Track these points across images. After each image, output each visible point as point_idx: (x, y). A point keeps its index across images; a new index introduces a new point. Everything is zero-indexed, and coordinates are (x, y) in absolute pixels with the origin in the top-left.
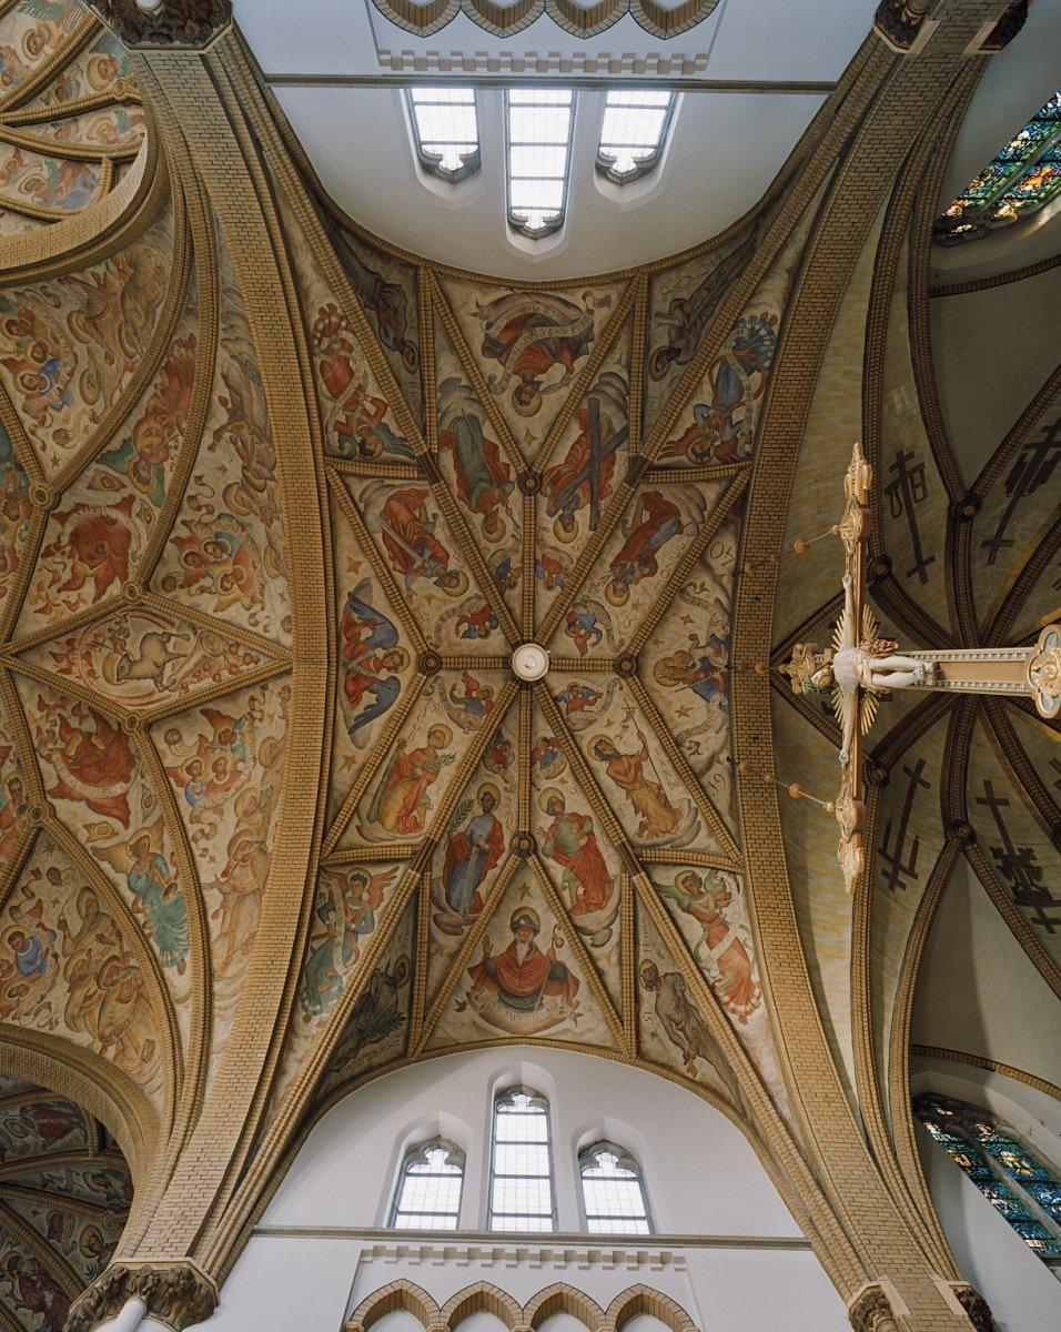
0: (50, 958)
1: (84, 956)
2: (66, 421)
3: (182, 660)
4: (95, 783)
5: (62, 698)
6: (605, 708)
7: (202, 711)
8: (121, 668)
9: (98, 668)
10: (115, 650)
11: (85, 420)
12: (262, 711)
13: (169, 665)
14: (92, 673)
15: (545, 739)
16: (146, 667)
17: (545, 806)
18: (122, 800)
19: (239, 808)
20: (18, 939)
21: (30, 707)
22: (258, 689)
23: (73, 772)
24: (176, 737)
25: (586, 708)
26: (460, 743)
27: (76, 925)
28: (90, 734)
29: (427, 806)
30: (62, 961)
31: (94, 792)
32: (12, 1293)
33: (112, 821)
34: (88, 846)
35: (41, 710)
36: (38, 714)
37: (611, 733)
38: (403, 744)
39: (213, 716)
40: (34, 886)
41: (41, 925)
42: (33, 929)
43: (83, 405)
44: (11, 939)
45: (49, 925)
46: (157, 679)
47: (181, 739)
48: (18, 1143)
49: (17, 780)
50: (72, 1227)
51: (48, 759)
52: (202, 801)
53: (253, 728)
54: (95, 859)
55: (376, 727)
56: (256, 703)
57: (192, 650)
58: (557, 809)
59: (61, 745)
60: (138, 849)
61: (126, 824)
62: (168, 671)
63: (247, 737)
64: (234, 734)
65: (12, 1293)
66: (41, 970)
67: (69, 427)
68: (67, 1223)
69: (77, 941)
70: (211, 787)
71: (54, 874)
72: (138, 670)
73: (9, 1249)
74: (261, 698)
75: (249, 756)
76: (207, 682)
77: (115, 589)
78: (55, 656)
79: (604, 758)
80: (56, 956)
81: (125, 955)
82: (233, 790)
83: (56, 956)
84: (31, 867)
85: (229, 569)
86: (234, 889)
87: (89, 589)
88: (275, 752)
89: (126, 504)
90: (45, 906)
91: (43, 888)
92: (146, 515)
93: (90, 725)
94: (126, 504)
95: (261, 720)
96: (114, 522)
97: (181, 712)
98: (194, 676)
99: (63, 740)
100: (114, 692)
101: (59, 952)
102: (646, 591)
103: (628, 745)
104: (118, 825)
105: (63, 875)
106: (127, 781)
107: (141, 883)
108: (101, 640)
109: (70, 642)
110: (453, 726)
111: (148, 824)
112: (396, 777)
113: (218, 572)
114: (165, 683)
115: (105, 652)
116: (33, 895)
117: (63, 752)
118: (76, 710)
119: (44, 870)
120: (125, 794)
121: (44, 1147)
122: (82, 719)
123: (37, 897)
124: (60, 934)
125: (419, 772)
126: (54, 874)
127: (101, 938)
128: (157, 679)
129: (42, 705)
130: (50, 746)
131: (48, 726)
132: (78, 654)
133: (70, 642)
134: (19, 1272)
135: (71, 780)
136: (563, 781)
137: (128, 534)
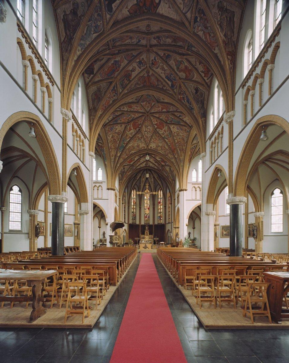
2: (175, 128)
11: (175, 131)
16: (147, 129)
27: (117, 131)
43: (176, 131)
46: (145, 131)
57: (149, 135)
60: (127, 135)
62: (146, 132)
67: (175, 129)
69: (116, 133)
72: (146, 128)
76: (145, 138)
77: (156, 127)
85: (157, 139)
87: (156, 123)
89: (165, 131)
92: (163, 134)
93: (139, 123)
94: (165, 131)
96: (163, 128)
100: (144, 127)
102: (153, 162)
103: (141, 161)
106: (133, 129)
113: (157, 138)
127: (117, 137)
128: (145, 131)
137: (162, 130)
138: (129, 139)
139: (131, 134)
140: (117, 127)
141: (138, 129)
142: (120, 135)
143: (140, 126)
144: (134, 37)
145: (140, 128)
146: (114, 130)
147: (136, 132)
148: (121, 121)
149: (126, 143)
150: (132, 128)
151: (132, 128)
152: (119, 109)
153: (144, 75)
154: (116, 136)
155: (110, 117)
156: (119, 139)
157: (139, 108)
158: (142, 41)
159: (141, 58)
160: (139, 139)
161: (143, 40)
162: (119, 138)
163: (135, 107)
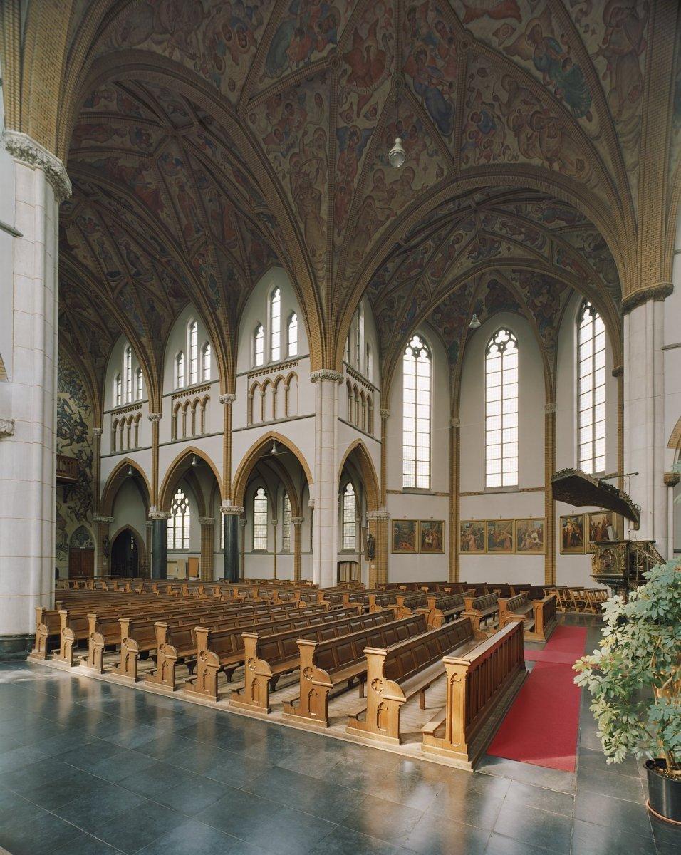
0: (496, 119)
20: (475, 117)
27: (504, 96)
30: (504, 120)
34: (501, 48)
41: (483, 103)
44: (472, 118)
45: (487, 101)
54: (509, 56)
66: (494, 128)
80: (498, 117)
83: (498, 117)
101: (499, 114)
105: (488, 71)
116: (474, 89)
123: (476, 88)
124: (496, 104)
140: (488, 97)
152: (369, 142)
155: (428, 144)
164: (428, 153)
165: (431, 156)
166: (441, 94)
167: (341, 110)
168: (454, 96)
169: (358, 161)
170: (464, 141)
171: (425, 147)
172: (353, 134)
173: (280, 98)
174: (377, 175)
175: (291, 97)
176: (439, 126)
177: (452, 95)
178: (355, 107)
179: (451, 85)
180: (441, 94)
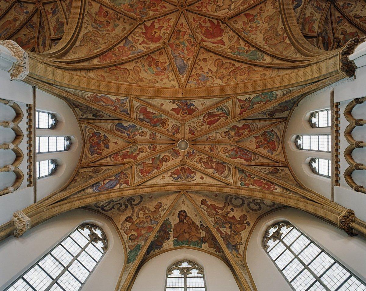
0: (208, 77)
1: (221, 74)
3: (237, 2)
4: (211, 38)
5: (200, 18)
6: (355, 7)
7: (244, 15)
8: (216, 9)
9: (209, 10)
10: (214, 4)
12: (264, 10)
13: (233, 5)
14: (208, 11)
15: (338, 17)
16: (225, 7)
17: (340, 33)
18: (222, 40)
19: (262, 33)
21: (192, 20)
22: (263, 4)
23: (204, 36)
24: (236, 22)
25: (349, 8)
26: (318, 16)
27: (214, 69)
28: (208, 27)
29: (315, 28)
31: (212, 40)
32: (202, 166)
33: (220, 45)
35: (194, 21)
36: (194, 23)
37: (358, 13)
38: (305, 15)
39: (247, 15)
40: (199, 63)
41: (203, 71)
42: (201, 73)
44: (196, 74)
45: (205, 71)
46: (229, 9)
47: (238, 23)
48: (199, 129)
49: (189, 39)
50: (217, 149)
51: (198, 33)
52: (249, 34)
53: (261, 16)
55: (299, 9)
56: (262, 9)
58: (344, 33)
59: (200, 30)
60: (230, 48)
61: (224, 45)
63: (259, 19)
64: (254, 19)
65: (202, 166)
68: (215, 148)
69: (217, 72)
70: (250, 31)
71: (205, 60)
73: (198, 157)
74: (264, 6)
75: (260, 22)
78: (198, 7)
79: (357, 18)
81: (238, 68)
82: (258, 30)
83: (211, 77)
84: (198, 58)
86: (271, 45)
88: (271, 18)
90: (203, 67)
91: (202, 64)
93: (208, 25)
95: (264, 13)
97: (238, 15)
98: (241, 5)
99: (200, 29)
101: (212, 76)
104: (222, 46)
105: (207, 59)
107: (237, 53)
108: (210, 2)
109: (202, 3)
110: (315, 12)
111: (232, 42)
112: (305, 22)
114: (232, 9)
115: (211, 5)
117: (201, 32)
118: (204, 21)
119: (201, 59)
120: (222, 39)
121: (209, 127)
122: (206, 23)
123: (200, 65)
124: (210, 72)
125: (310, 21)
126: (205, 60)
127: (226, 68)
129: (194, 20)
130: (198, 30)
131: (196, 25)
132: (204, 6)
133: (202, 3)
134: (203, 162)
135: (204, 38)
136: (345, 26)
138: (241, 42)
139: (230, 38)
140: (206, 70)
141: (222, 26)
142: (225, 61)
143: (215, 22)
144: (16, 16)
145: (218, 20)
146: (210, 74)
147: (228, 29)
148: (189, 59)
149: (247, 48)
150: (219, 38)
151: (219, 38)
153: (67, 4)
154: (225, 71)
156: (233, 62)
157: (166, 25)
158: (28, 10)
159: (50, 11)
160: (250, 21)
161: (27, 9)
162: (230, 63)
163: (163, 31)
164: (168, 80)
165: (170, 81)
166: (183, 61)
167: (133, 36)
168: (190, 62)
169: (130, 54)
170: (190, 80)
171: (168, 77)
172: (133, 46)
173: (107, 15)
174: (136, 68)
175: (112, 21)
176: (178, 70)
177: (188, 62)
178: (140, 42)
179: (189, 59)
180: (183, 61)
